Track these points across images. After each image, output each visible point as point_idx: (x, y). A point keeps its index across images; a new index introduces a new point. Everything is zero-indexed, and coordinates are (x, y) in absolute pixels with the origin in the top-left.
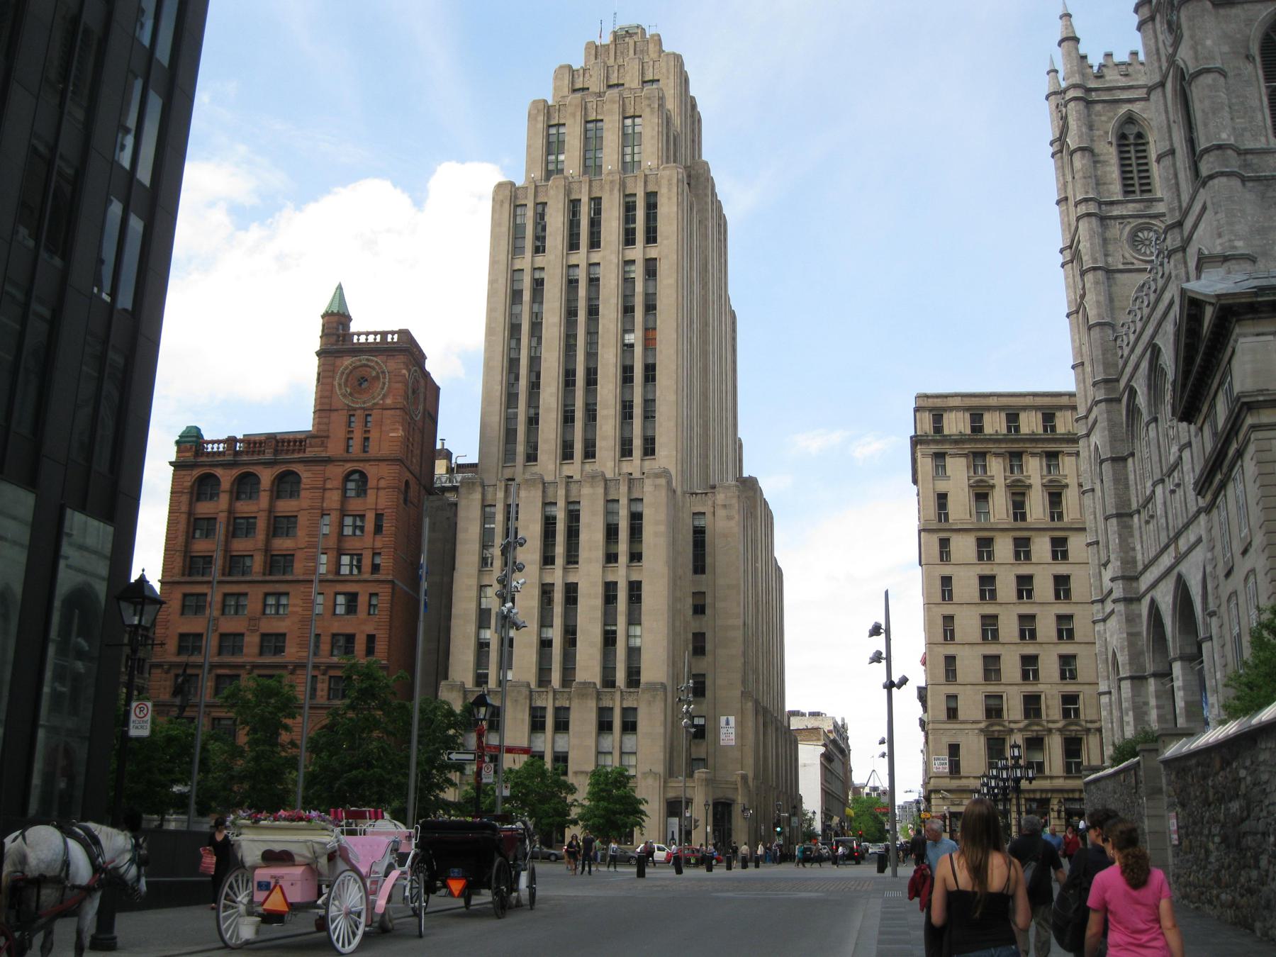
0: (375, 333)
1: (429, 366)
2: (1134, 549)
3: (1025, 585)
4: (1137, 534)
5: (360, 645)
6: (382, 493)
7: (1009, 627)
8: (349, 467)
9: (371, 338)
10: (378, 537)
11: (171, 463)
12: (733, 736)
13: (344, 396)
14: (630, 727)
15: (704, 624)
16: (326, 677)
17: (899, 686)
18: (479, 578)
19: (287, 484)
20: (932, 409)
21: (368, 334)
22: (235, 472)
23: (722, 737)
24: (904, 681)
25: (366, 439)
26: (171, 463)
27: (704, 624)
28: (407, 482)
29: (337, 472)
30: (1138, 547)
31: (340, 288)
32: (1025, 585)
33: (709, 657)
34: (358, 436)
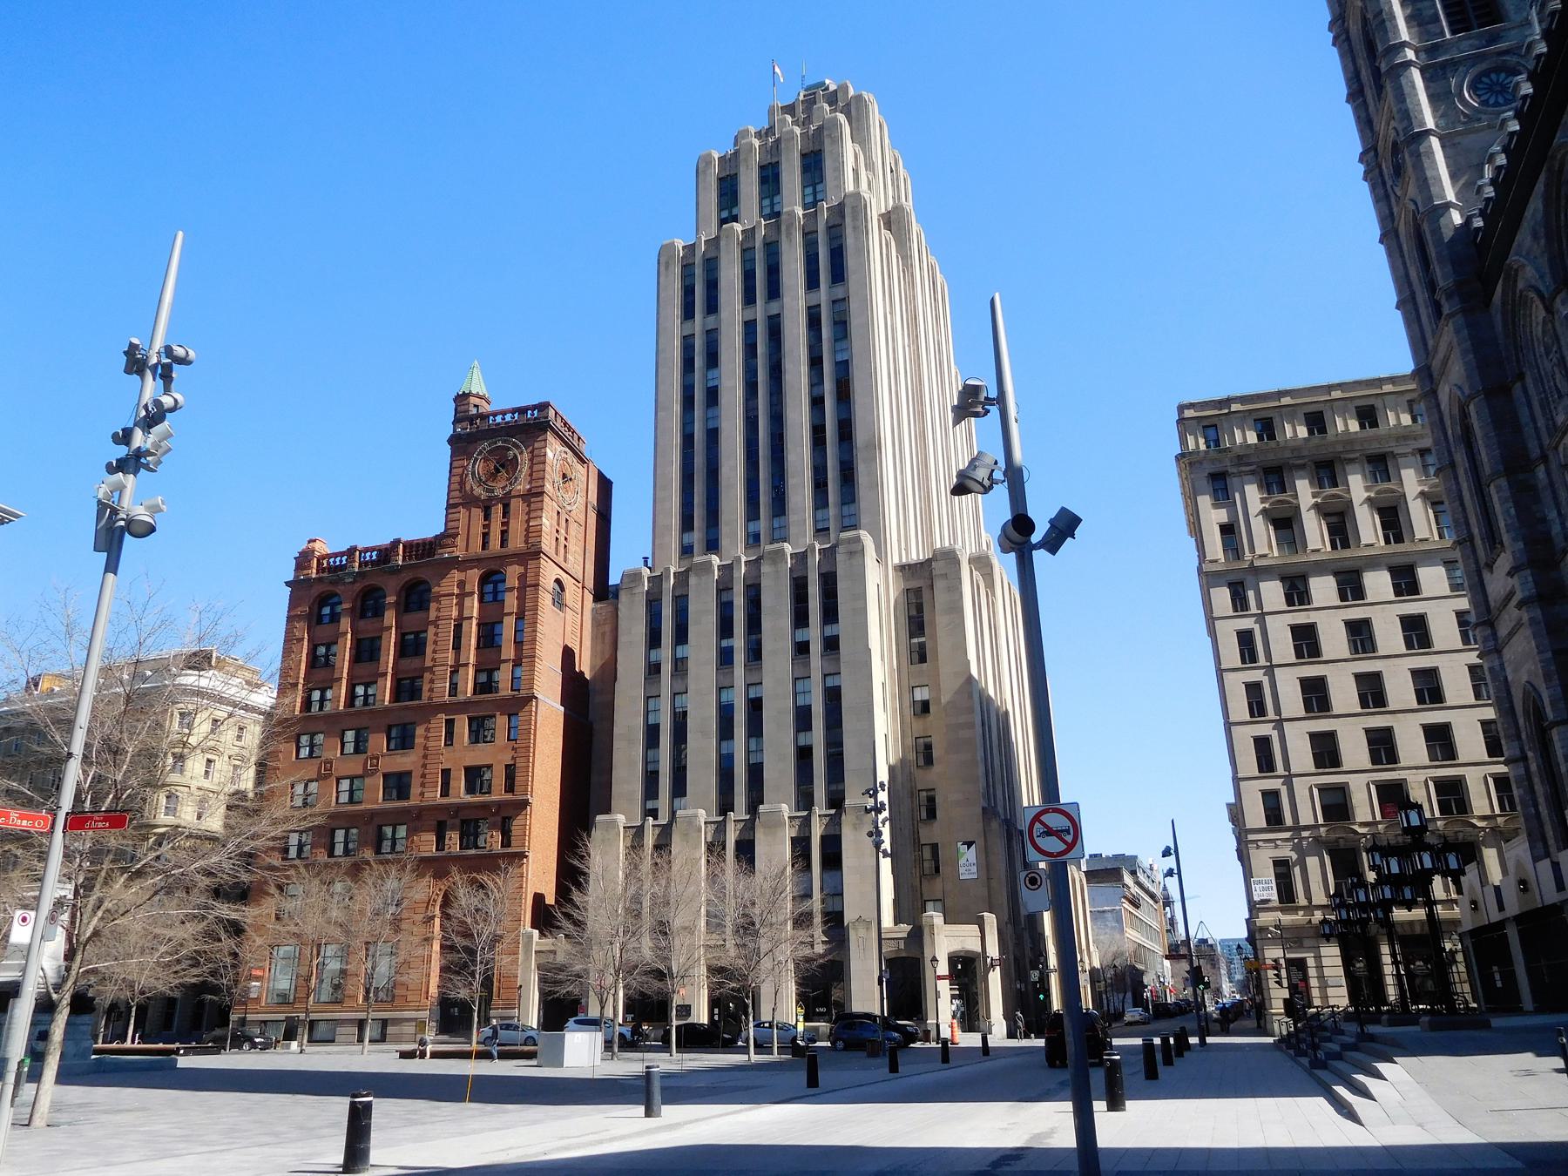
0: (513, 411)
2: (1544, 520)
3: (1360, 634)
4: (1546, 496)
5: (499, 780)
7: (1344, 694)
9: (508, 417)
11: (288, 584)
12: (974, 869)
16: (457, 821)
17: (1053, 543)
19: (416, 597)
20: (1204, 420)
21: (504, 413)
23: (962, 870)
24: (1065, 526)
26: (288, 584)
28: (558, 581)
30: (1553, 515)
32: (1360, 634)
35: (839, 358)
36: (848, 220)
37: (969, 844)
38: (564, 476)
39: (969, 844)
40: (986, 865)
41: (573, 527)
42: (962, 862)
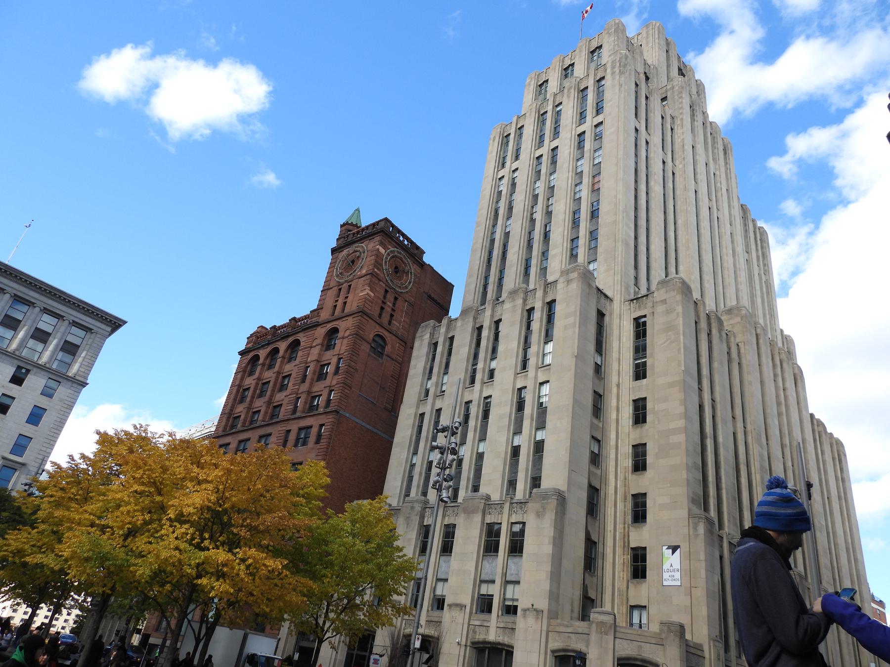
1: (426, 259)
6: (345, 341)
8: (329, 326)
10: (337, 377)
12: (677, 575)
13: (337, 276)
14: (516, 548)
15: (649, 434)
18: (418, 407)
22: (269, 349)
23: (666, 575)
25: (345, 303)
27: (649, 434)
29: (321, 332)
31: (358, 210)
33: (650, 472)
34: (340, 304)
35: (596, 162)
36: (609, 70)
37: (674, 549)
38: (396, 268)
39: (674, 549)
40: (688, 572)
41: (402, 306)
42: (666, 566)
